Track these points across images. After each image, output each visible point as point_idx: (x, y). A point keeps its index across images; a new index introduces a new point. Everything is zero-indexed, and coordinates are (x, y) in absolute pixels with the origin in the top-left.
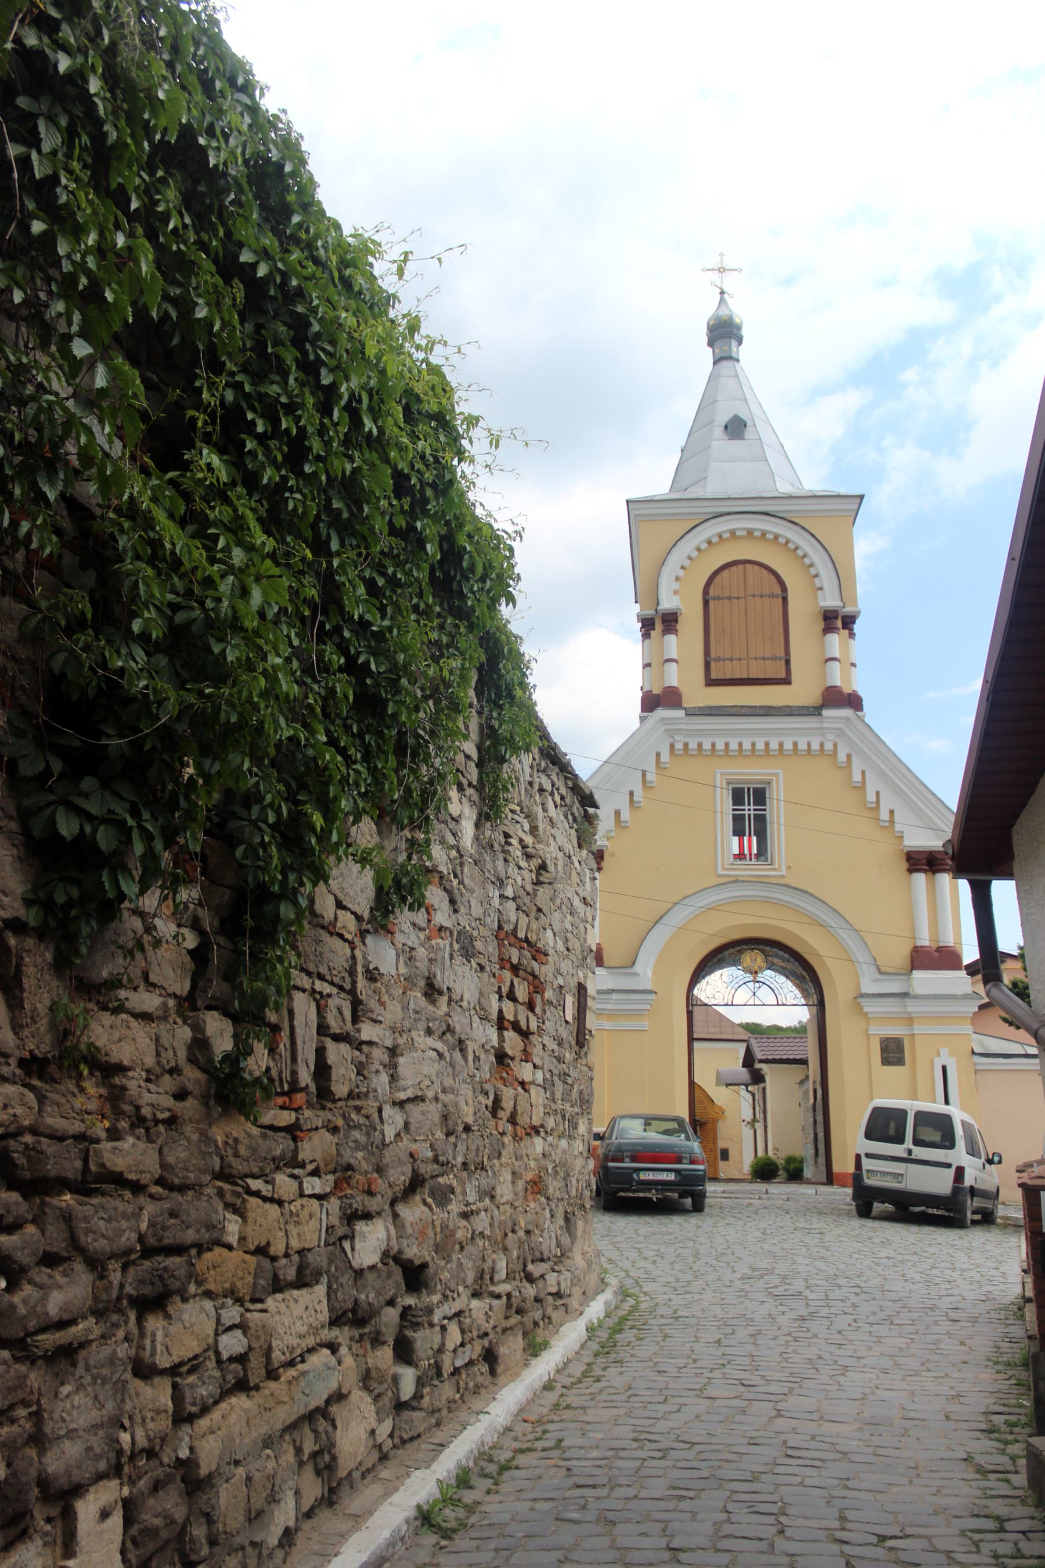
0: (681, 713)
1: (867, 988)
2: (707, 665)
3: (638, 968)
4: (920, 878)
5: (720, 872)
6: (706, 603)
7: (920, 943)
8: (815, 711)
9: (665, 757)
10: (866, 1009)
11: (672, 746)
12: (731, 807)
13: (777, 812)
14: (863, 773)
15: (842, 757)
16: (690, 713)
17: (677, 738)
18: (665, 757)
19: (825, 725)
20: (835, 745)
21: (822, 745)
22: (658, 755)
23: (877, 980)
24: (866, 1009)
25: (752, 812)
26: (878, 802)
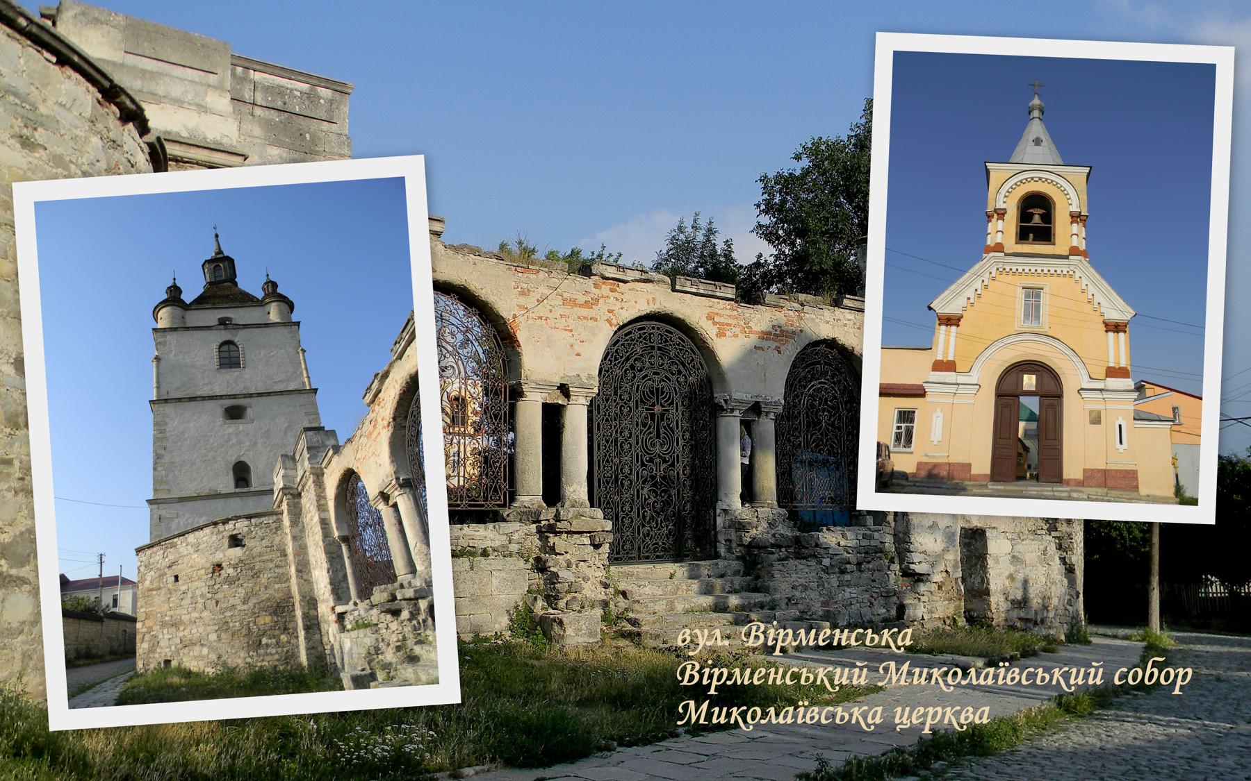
4: (1111, 334)
7: (1112, 365)
8: (1066, 257)
13: (1045, 299)
16: (1006, 255)
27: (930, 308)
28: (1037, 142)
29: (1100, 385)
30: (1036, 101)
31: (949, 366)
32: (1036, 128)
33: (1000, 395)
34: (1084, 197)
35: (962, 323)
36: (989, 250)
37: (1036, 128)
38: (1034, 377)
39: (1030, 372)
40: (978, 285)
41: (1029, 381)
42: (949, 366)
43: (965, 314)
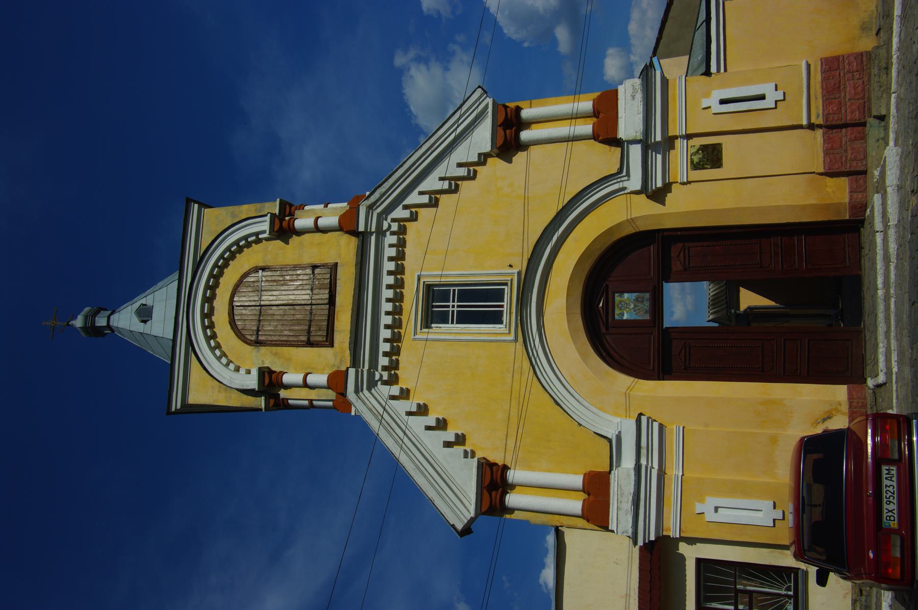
0: (352, 372)
1: (635, 182)
2: (310, 344)
3: (611, 433)
5: (512, 337)
6: (258, 343)
9: (395, 390)
10: (659, 184)
11: (385, 383)
12: (450, 325)
14: (421, 193)
15: (406, 214)
17: (377, 377)
18: (395, 390)
19: (373, 229)
20: (394, 220)
21: (393, 233)
22: (393, 398)
23: (628, 175)
24: (659, 184)
25: (456, 304)
26: (450, 179)
27: (467, 530)
28: (145, 314)
29: (635, 152)
30: (78, 322)
31: (596, 488)
32: (125, 319)
33: (664, 371)
34: (246, 210)
35: (496, 457)
36: (342, 403)
37: (125, 319)
38: (617, 298)
39: (610, 306)
40: (417, 424)
41: (629, 307)
42: (596, 488)
43: (479, 454)
